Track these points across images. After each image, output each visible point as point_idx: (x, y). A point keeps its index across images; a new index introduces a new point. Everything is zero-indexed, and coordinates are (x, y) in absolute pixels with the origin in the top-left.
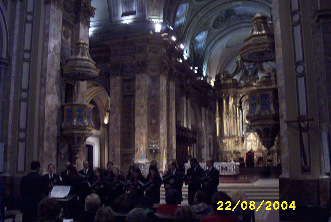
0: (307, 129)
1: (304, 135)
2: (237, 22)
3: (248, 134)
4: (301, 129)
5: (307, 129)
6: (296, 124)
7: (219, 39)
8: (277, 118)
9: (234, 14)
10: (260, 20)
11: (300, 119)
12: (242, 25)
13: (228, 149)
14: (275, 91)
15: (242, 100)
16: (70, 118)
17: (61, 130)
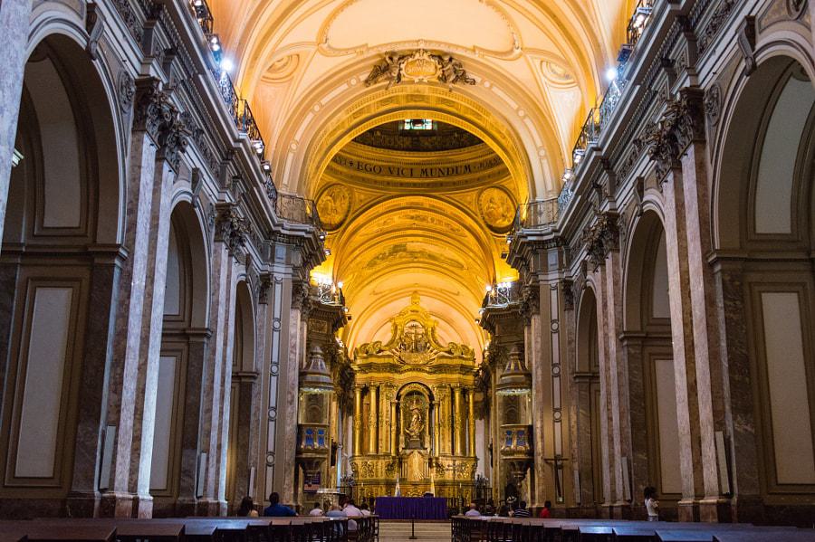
0: (561, 467)
1: (560, 471)
2: (404, 260)
3: (408, 451)
4: (557, 467)
5: (561, 467)
6: (553, 462)
7: (367, 284)
8: (531, 453)
9: (405, 250)
10: (517, 357)
11: (557, 458)
12: (411, 265)
13: (374, 478)
14: (531, 429)
15: (402, 393)
16: (310, 440)
17: (299, 452)
